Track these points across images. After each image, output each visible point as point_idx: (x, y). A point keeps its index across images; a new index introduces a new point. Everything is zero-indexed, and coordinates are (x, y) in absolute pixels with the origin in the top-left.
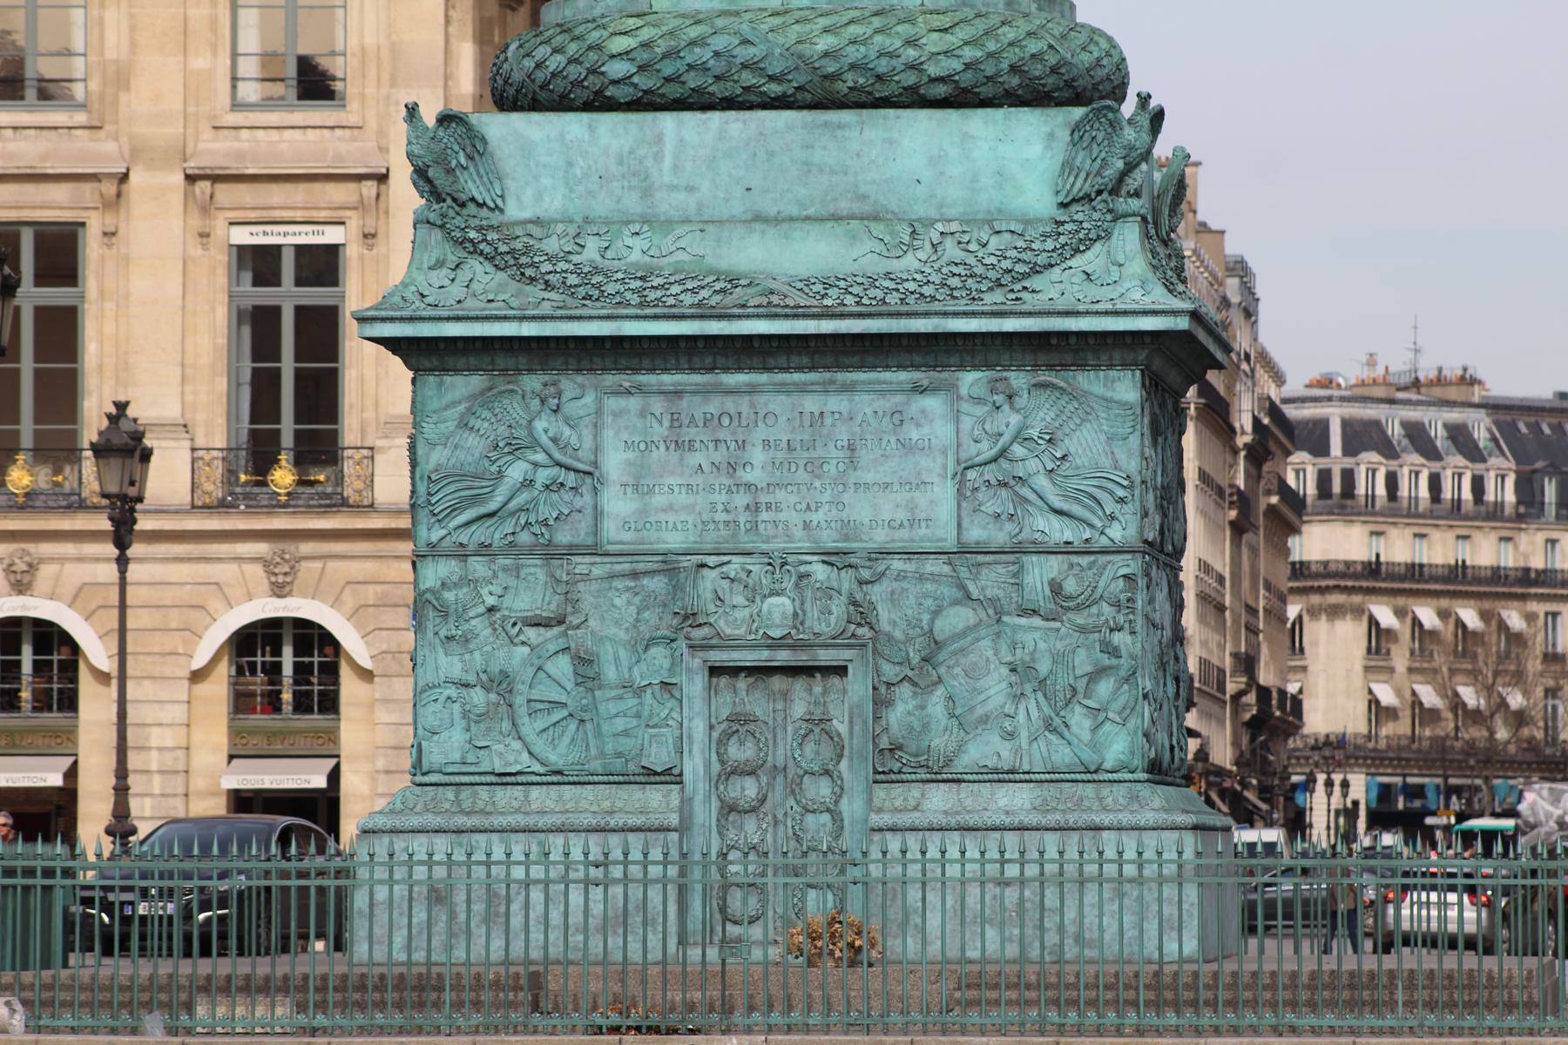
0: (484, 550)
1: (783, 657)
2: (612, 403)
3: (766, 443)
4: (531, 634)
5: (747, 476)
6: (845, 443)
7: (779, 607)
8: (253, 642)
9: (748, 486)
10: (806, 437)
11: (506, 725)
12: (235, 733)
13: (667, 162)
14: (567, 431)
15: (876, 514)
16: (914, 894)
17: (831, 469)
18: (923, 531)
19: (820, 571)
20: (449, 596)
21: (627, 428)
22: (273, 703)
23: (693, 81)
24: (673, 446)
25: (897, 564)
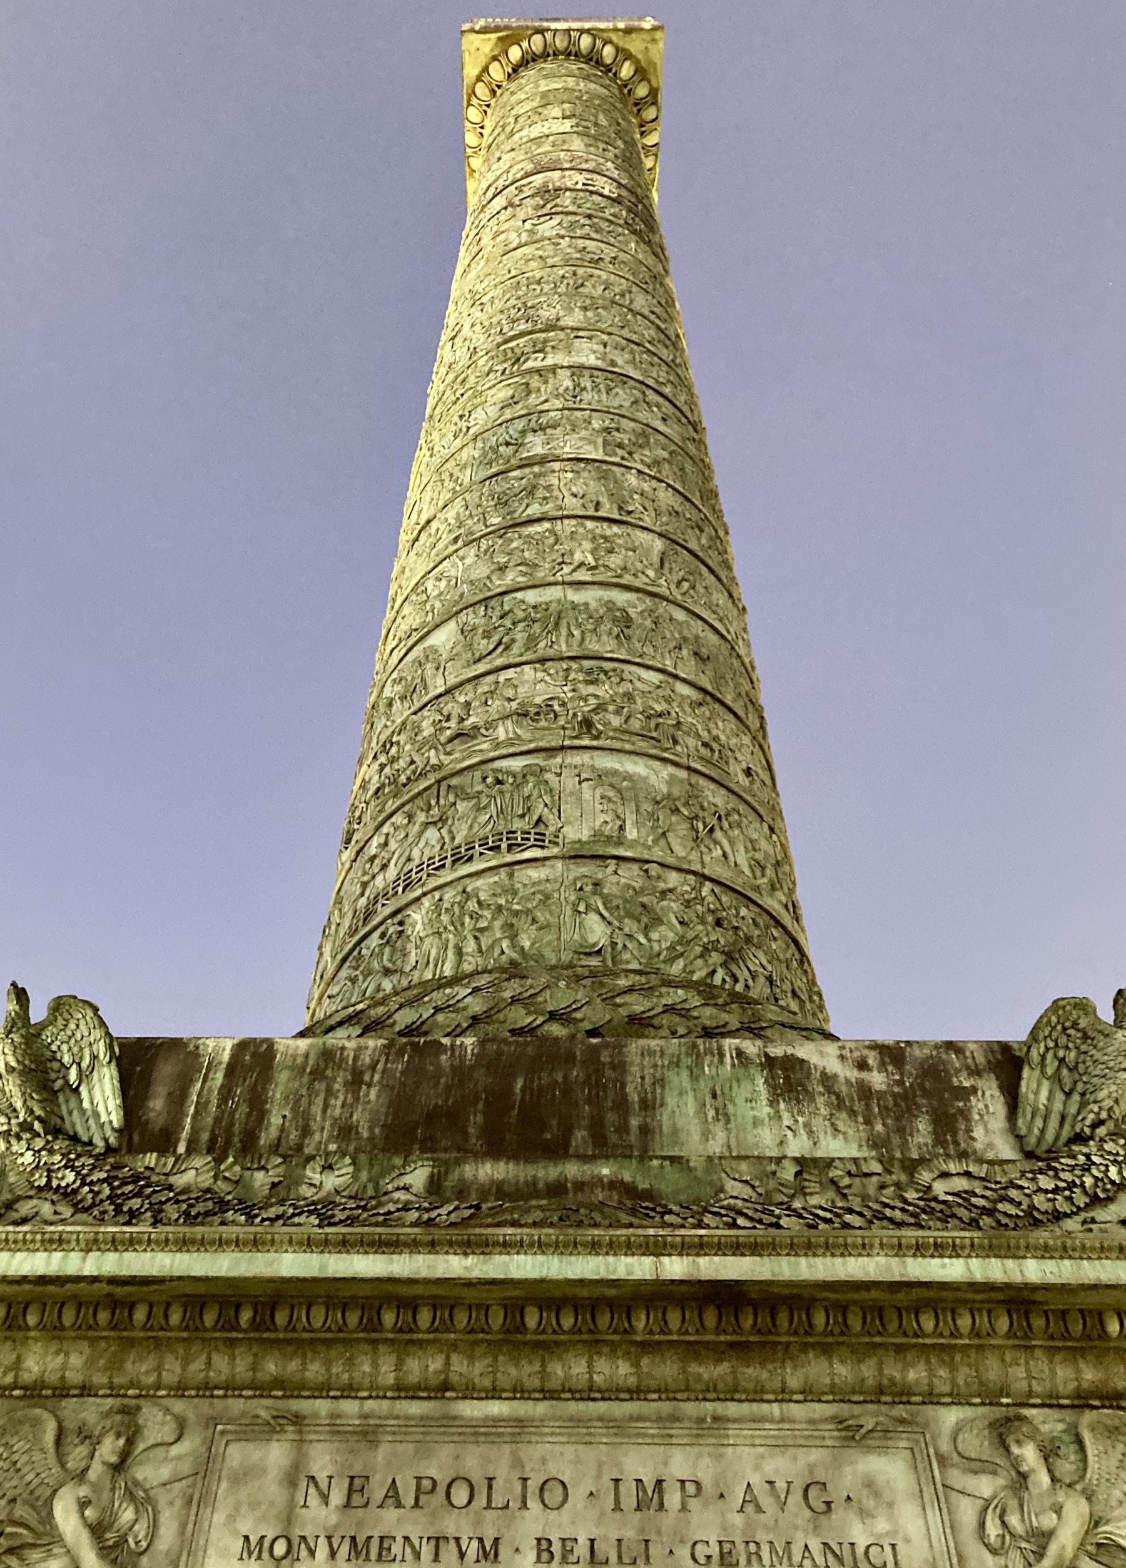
6: (714, 1550)
10: (630, 1534)
14: (128, 1515)
21: (254, 1505)
24: (345, 1548)
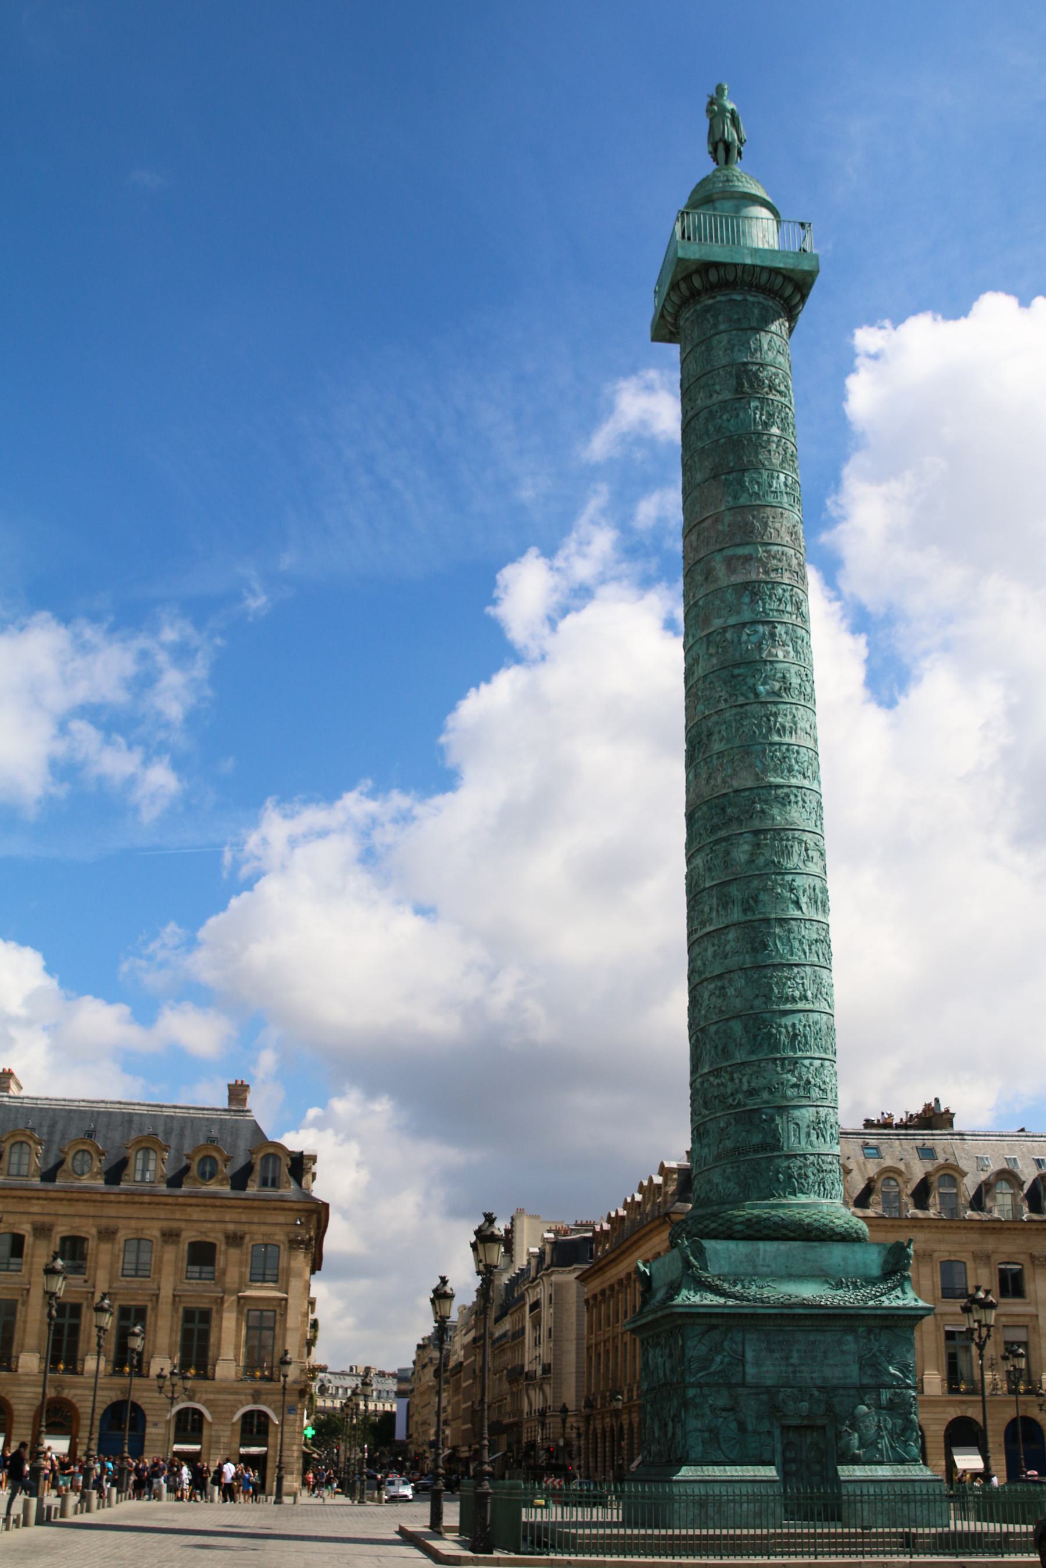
0: (707, 1385)
1: (805, 1422)
2: (748, 1336)
3: (798, 1351)
4: (724, 1414)
5: (792, 1361)
7: (805, 1405)
8: (247, 1416)
9: (792, 1365)
11: (716, 1445)
12: (242, 1438)
13: (761, 1257)
15: (833, 1373)
16: (859, 1505)
17: (819, 1359)
18: (848, 1380)
19: (816, 1393)
20: (697, 1400)
22: (251, 1431)
23: (765, 1232)
25: (841, 1391)
